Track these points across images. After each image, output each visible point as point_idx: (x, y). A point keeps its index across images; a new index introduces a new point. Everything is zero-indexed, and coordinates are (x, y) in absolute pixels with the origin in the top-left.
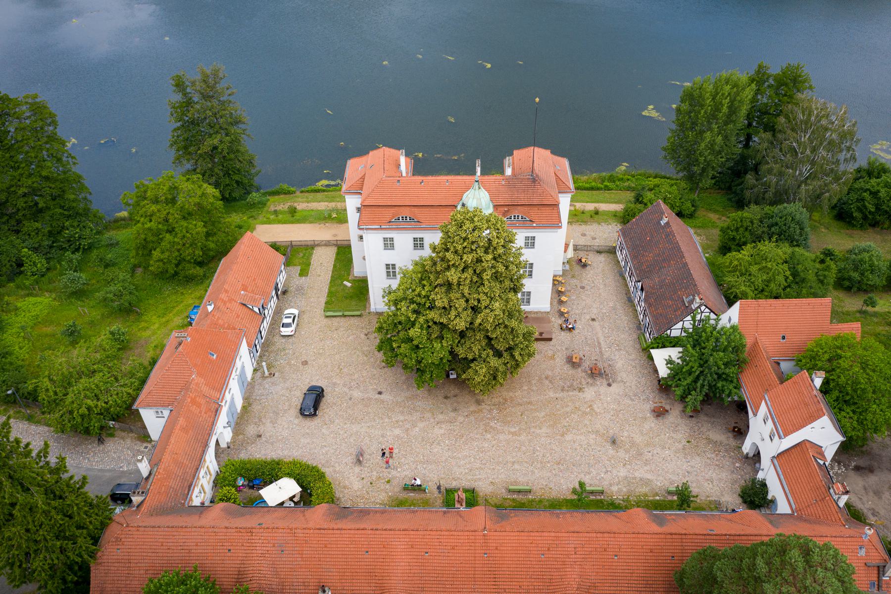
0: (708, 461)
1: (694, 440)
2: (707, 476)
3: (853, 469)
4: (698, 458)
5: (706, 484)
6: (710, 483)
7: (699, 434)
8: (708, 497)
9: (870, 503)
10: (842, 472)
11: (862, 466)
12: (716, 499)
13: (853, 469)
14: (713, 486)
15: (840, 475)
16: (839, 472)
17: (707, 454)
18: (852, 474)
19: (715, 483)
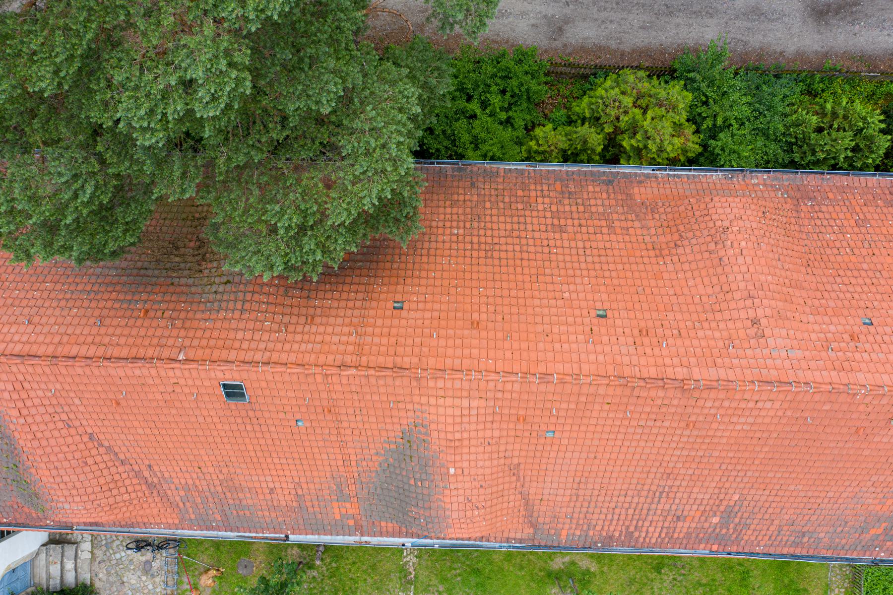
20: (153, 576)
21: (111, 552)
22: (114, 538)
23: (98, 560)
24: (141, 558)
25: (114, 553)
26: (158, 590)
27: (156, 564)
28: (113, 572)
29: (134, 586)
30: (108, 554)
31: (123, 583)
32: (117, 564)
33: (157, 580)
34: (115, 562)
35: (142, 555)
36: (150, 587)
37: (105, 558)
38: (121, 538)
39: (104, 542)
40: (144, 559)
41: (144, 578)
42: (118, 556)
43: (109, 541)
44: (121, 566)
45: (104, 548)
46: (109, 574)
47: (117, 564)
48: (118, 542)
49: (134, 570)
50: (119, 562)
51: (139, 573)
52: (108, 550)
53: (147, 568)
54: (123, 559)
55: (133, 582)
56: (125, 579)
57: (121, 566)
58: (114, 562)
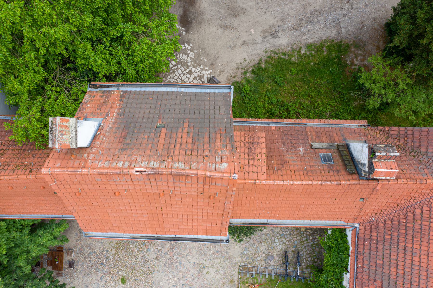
0: (163, 260)
1: (120, 270)
2: (192, 271)
3: (187, 31)
4: (157, 276)
5: (208, 277)
6: (206, 270)
7: (107, 258)
8: (232, 281)
9: (252, 31)
10: (192, 50)
11: (181, 13)
12: (237, 270)
13: (187, 31)
14: (212, 267)
15: (198, 56)
16: (191, 55)
17: (150, 258)
18: (193, 36)
19: (207, 263)
20: (265, 260)
21: (279, 237)
22: (287, 239)
23: (274, 229)
24: (275, 254)
25: (278, 239)
26: (257, 263)
27: (272, 262)
28: (267, 237)
29: (259, 249)
30: (278, 235)
31: (261, 243)
32: (272, 240)
33: (263, 263)
34: (273, 239)
35: (277, 255)
36: (259, 259)
37: (275, 233)
38: (287, 243)
39: (284, 233)
40: (275, 255)
41: (264, 255)
42: (277, 241)
43: (285, 236)
44: (271, 242)
45: (281, 233)
46: (266, 235)
47: (272, 240)
48: (285, 241)
49: (268, 249)
50: (273, 241)
51: (266, 253)
52: (280, 235)
53: (268, 256)
54: (275, 244)
55: (262, 249)
56: (263, 244)
57: (271, 242)
58: (273, 238)
